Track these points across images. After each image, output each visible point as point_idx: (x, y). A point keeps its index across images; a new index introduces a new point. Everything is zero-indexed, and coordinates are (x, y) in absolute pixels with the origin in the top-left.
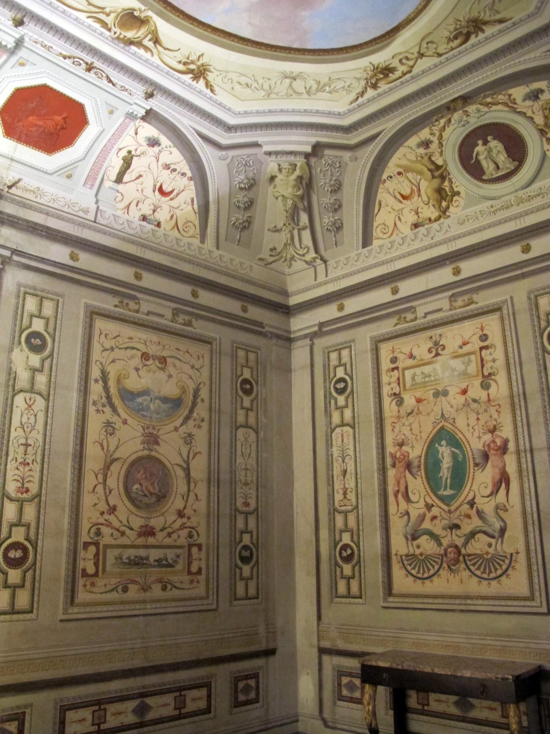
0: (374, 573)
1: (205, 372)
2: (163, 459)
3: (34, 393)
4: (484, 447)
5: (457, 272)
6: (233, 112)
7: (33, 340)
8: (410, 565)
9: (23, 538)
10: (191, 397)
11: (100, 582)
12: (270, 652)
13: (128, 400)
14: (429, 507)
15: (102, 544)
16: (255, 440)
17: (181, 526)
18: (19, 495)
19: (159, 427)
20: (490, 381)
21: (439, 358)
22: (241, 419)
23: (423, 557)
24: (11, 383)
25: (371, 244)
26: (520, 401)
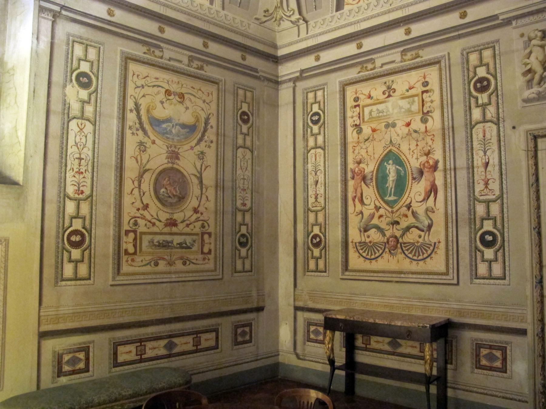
0: (335, 254)
2: (182, 170)
3: (84, 119)
4: (420, 165)
5: (408, 32)
7: (81, 79)
8: (362, 249)
9: (81, 227)
10: (203, 125)
11: (138, 259)
12: (260, 309)
13: (156, 126)
14: (377, 208)
15: (138, 231)
16: (250, 157)
18: (77, 196)
19: (179, 147)
20: (429, 118)
21: (391, 98)
22: (240, 142)
23: (372, 244)
24: (66, 112)
25: (343, 9)
26: (449, 133)
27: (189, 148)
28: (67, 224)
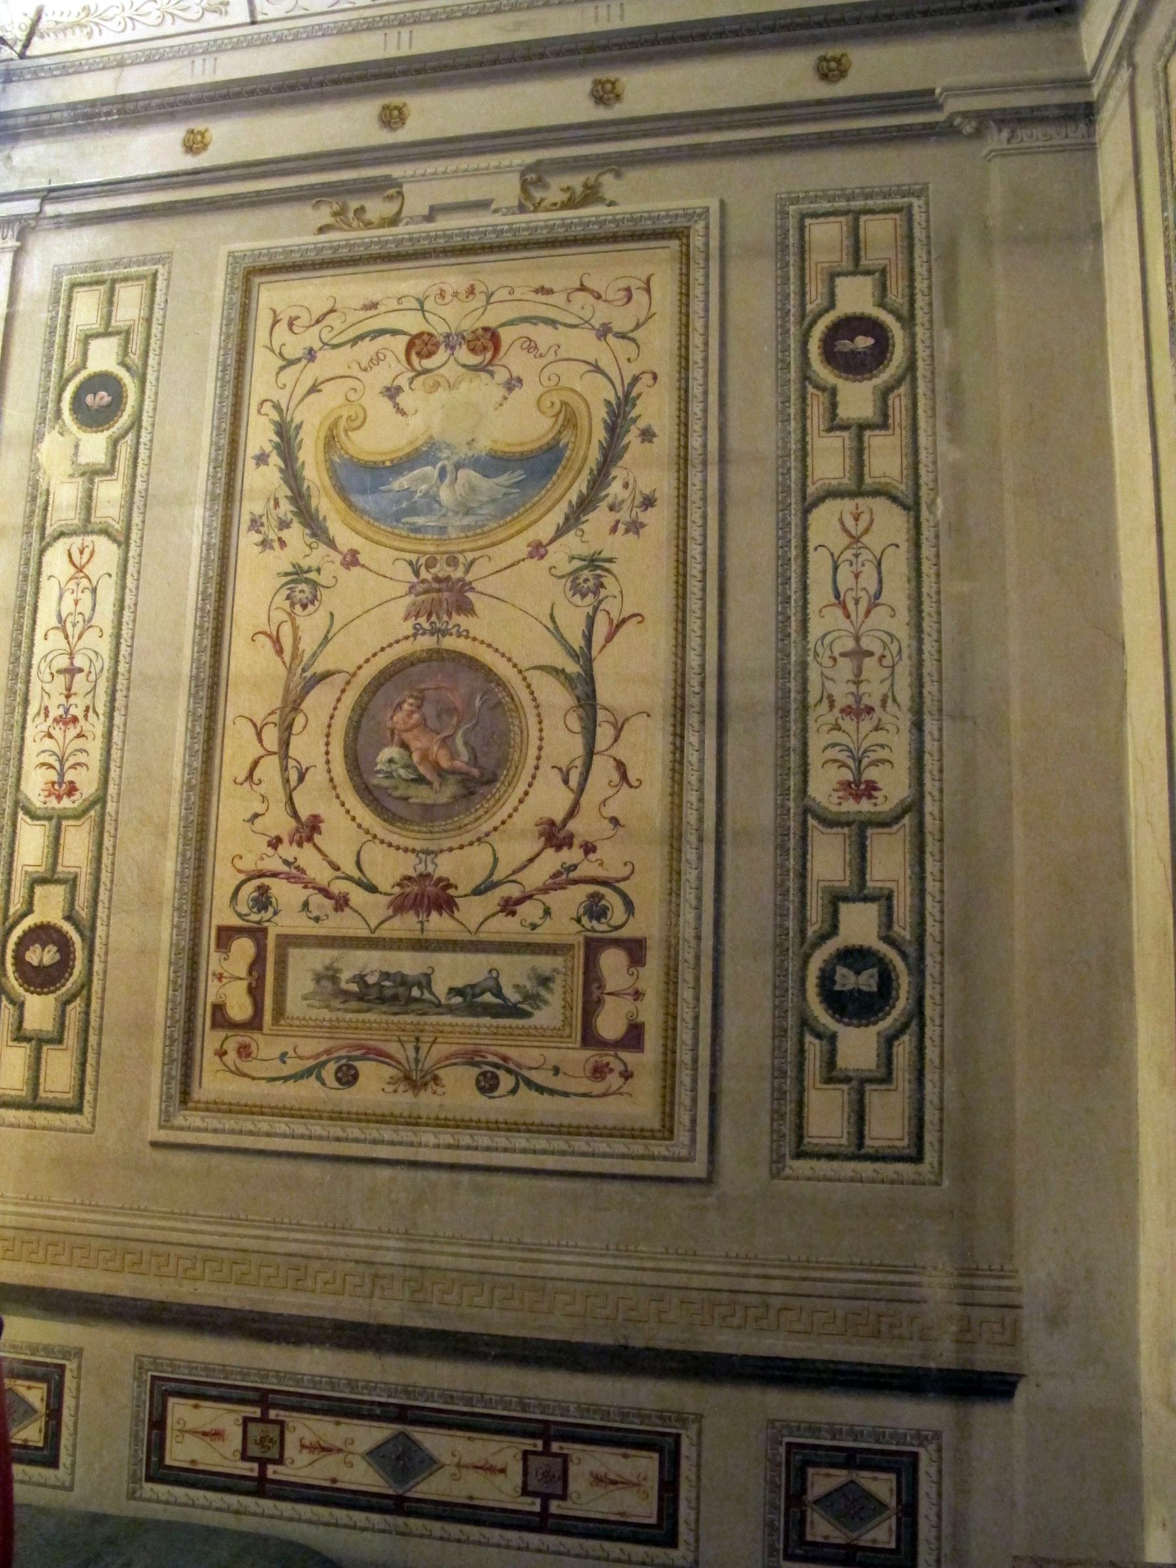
1: (659, 342)
2: (487, 657)
3: (92, 532)
7: (89, 399)
9: (60, 914)
11: (267, 1046)
13: (363, 492)
17: (555, 876)
18: (53, 803)
19: (470, 556)
24: (37, 520)
27: (525, 551)
28: (16, 907)
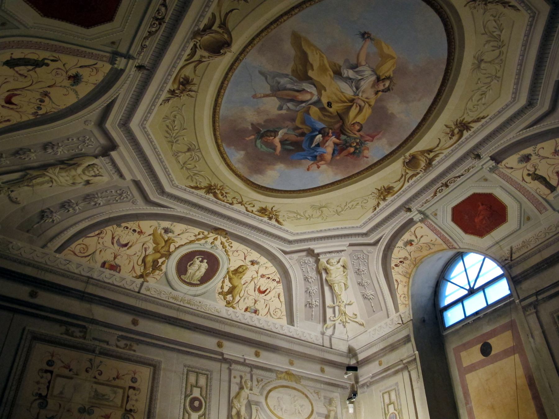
6: (511, 103)
